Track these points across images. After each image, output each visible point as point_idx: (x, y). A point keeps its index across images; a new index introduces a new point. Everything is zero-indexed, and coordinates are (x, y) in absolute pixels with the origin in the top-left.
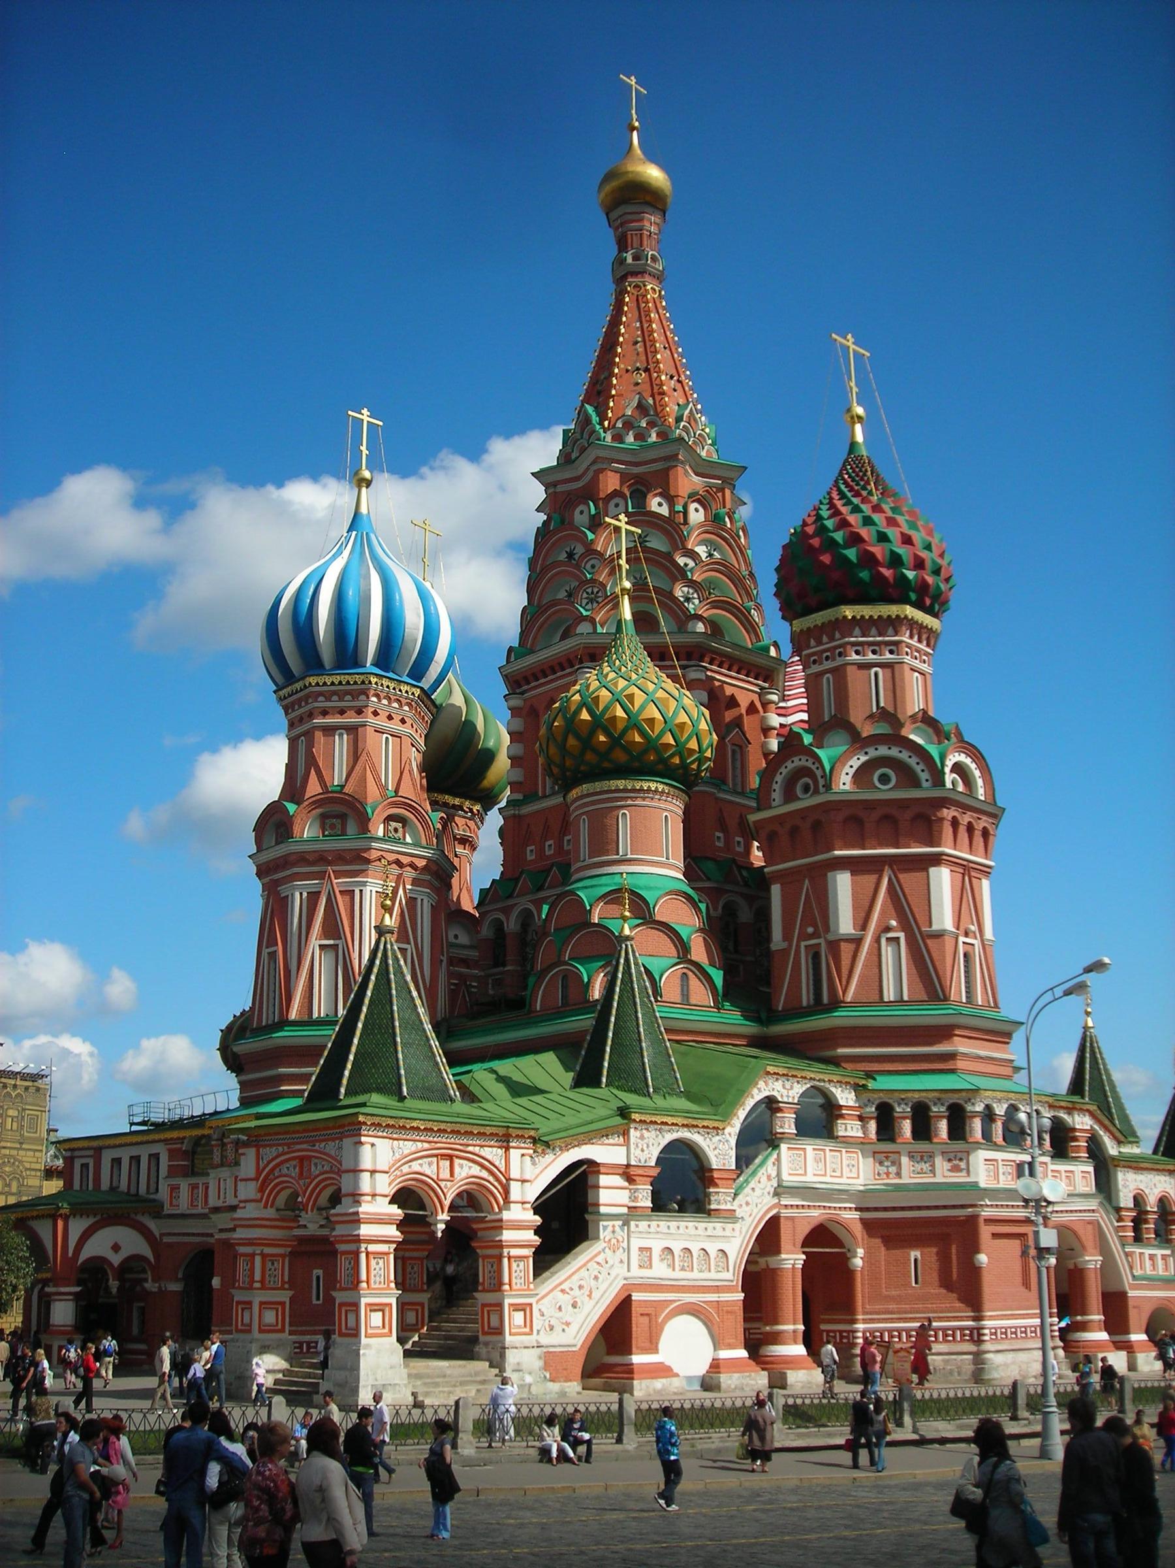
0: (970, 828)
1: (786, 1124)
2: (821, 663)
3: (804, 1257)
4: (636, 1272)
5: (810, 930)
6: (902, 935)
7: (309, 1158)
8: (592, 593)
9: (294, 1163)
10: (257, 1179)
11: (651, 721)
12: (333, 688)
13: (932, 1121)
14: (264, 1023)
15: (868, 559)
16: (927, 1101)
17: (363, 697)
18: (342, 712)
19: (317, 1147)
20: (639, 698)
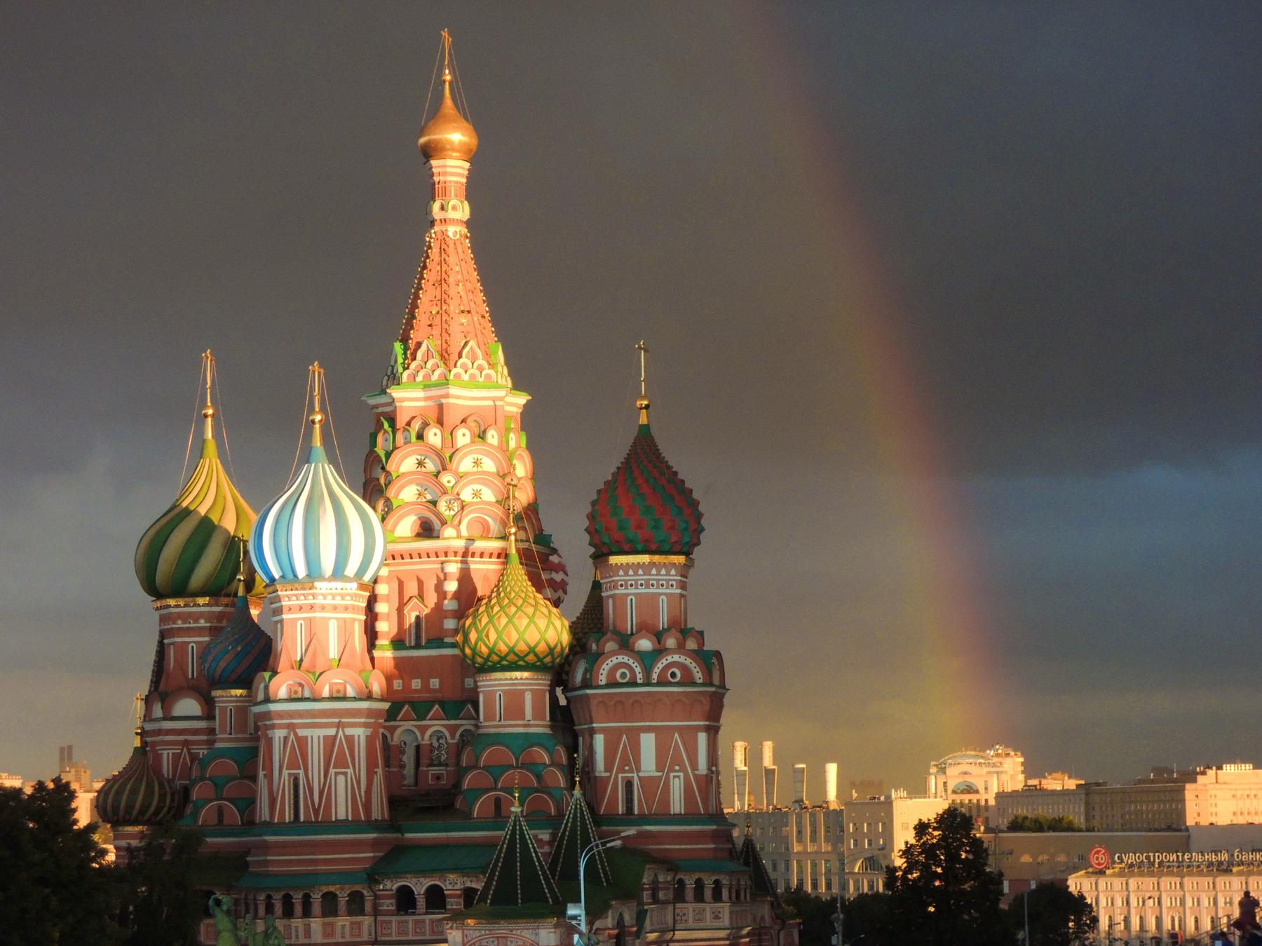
1: (646, 897)
2: (626, 588)
5: (627, 768)
6: (682, 775)
7: (505, 937)
12: (331, 591)
17: (348, 598)
18: (335, 608)
19: (514, 932)
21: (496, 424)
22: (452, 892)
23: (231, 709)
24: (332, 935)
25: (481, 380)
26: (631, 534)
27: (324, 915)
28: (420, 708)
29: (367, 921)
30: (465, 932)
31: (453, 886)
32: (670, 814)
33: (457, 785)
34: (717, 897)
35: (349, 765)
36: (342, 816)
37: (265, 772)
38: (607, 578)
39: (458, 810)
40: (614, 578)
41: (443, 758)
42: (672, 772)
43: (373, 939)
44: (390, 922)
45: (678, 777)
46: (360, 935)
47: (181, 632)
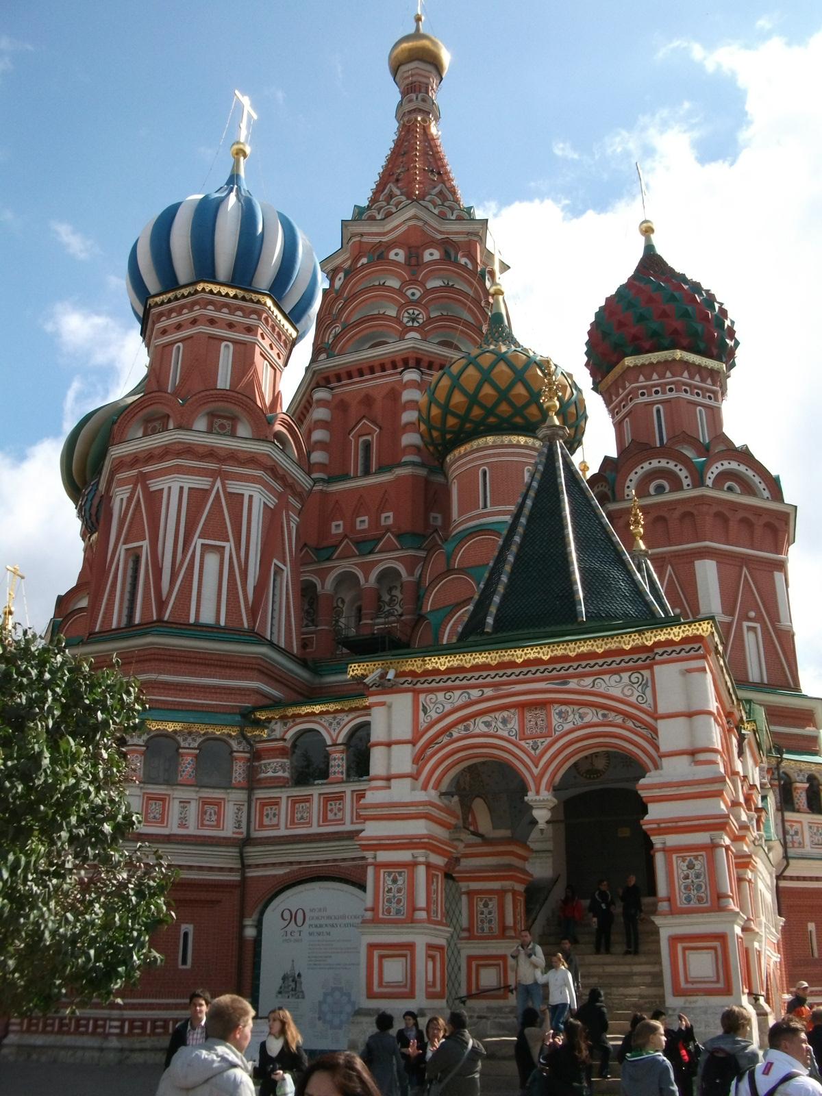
2: (650, 395)
7: (543, 705)
8: (413, 313)
9: (505, 714)
10: (413, 743)
14: (114, 627)
18: (231, 326)
19: (573, 684)
24: (162, 819)
25: (453, 218)
26: (654, 325)
27: (148, 780)
28: (366, 544)
29: (232, 802)
32: (747, 681)
35: (228, 536)
36: (207, 617)
38: (618, 395)
41: (396, 613)
42: (745, 621)
44: (276, 802)
46: (218, 826)
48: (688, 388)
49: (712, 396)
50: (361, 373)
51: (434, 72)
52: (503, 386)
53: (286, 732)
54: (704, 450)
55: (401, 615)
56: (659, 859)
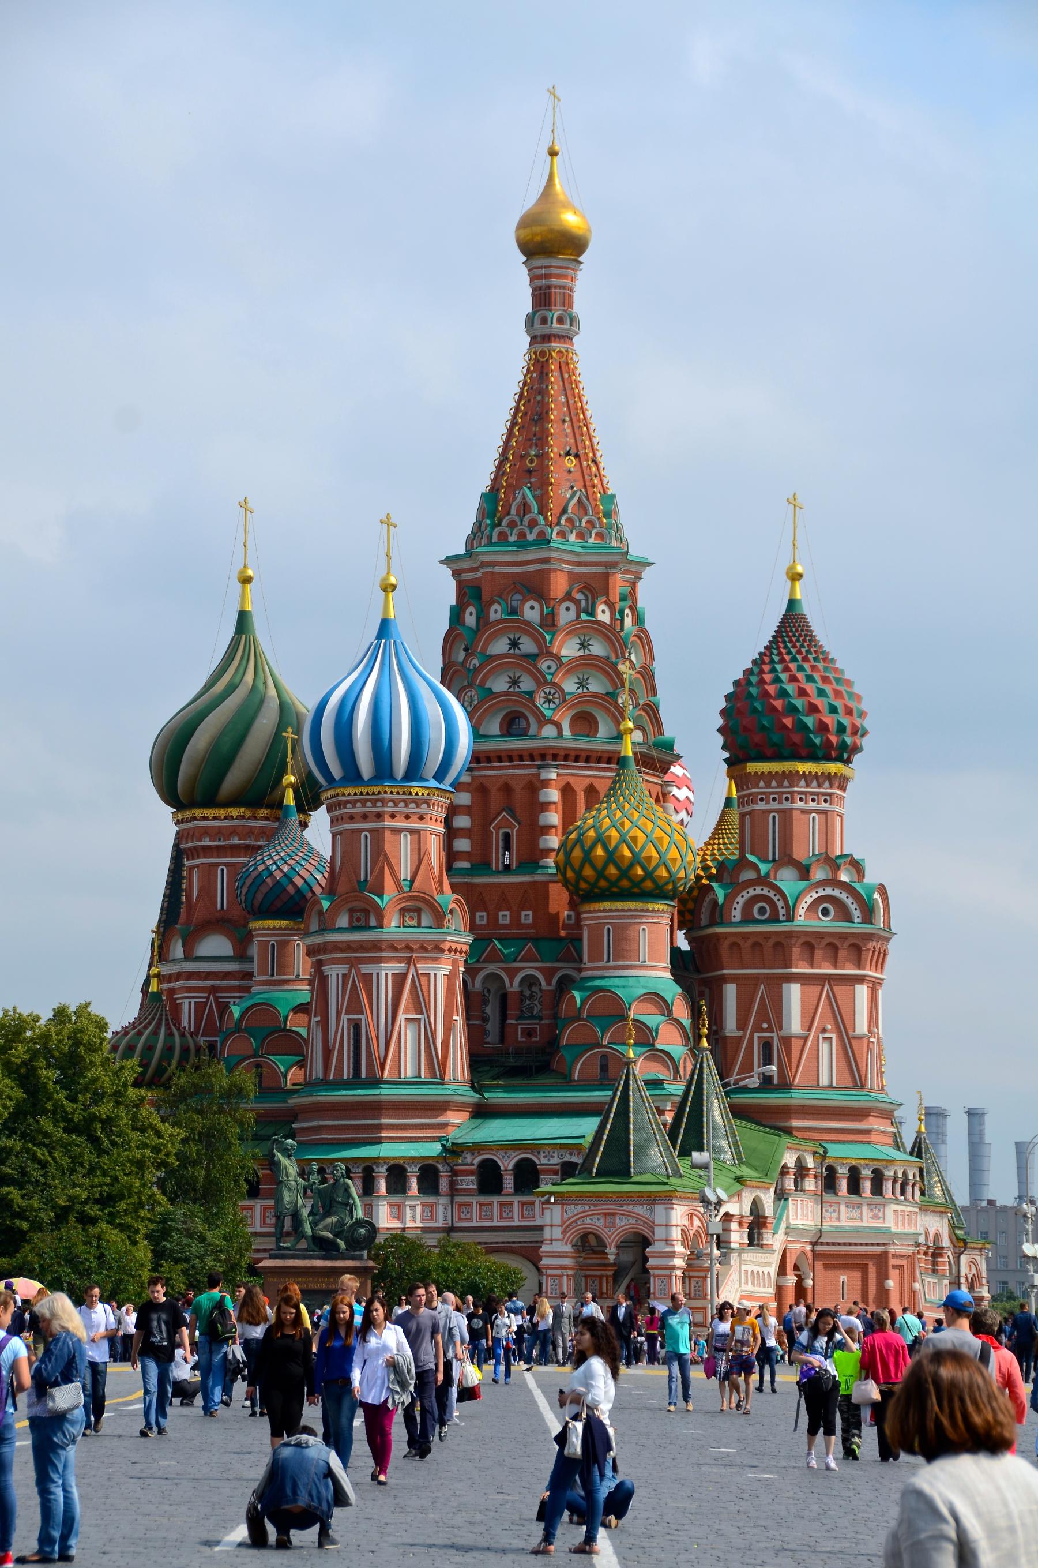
0: (880, 953)
1: (789, 1183)
3: (796, 1278)
4: (744, 1287)
5: (765, 1026)
6: (834, 1036)
7: (614, 1214)
11: (674, 860)
13: (861, 1181)
14: (345, 1077)
15: (823, 728)
16: (859, 1166)
17: (424, 806)
18: (407, 817)
19: (625, 1208)
20: (666, 839)
21: (607, 597)
22: (547, 1167)
23: (273, 945)
24: (399, 1216)
26: (776, 738)
29: (442, 1203)
30: (565, 1206)
31: (549, 1160)
33: (553, 1043)
34: (877, 1189)
37: (318, 1019)
38: (743, 790)
39: (553, 1070)
40: (754, 790)
41: (535, 1012)
43: (450, 1225)
44: (469, 1205)
45: (831, 1038)
46: (432, 1219)
47: (206, 851)
48: (803, 796)
49: (828, 798)
50: (500, 759)
51: (572, 265)
52: (625, 864)
53: (473, 1160)
54: (804, 872)
55: (541, 1019)
56: (652, 1278)
